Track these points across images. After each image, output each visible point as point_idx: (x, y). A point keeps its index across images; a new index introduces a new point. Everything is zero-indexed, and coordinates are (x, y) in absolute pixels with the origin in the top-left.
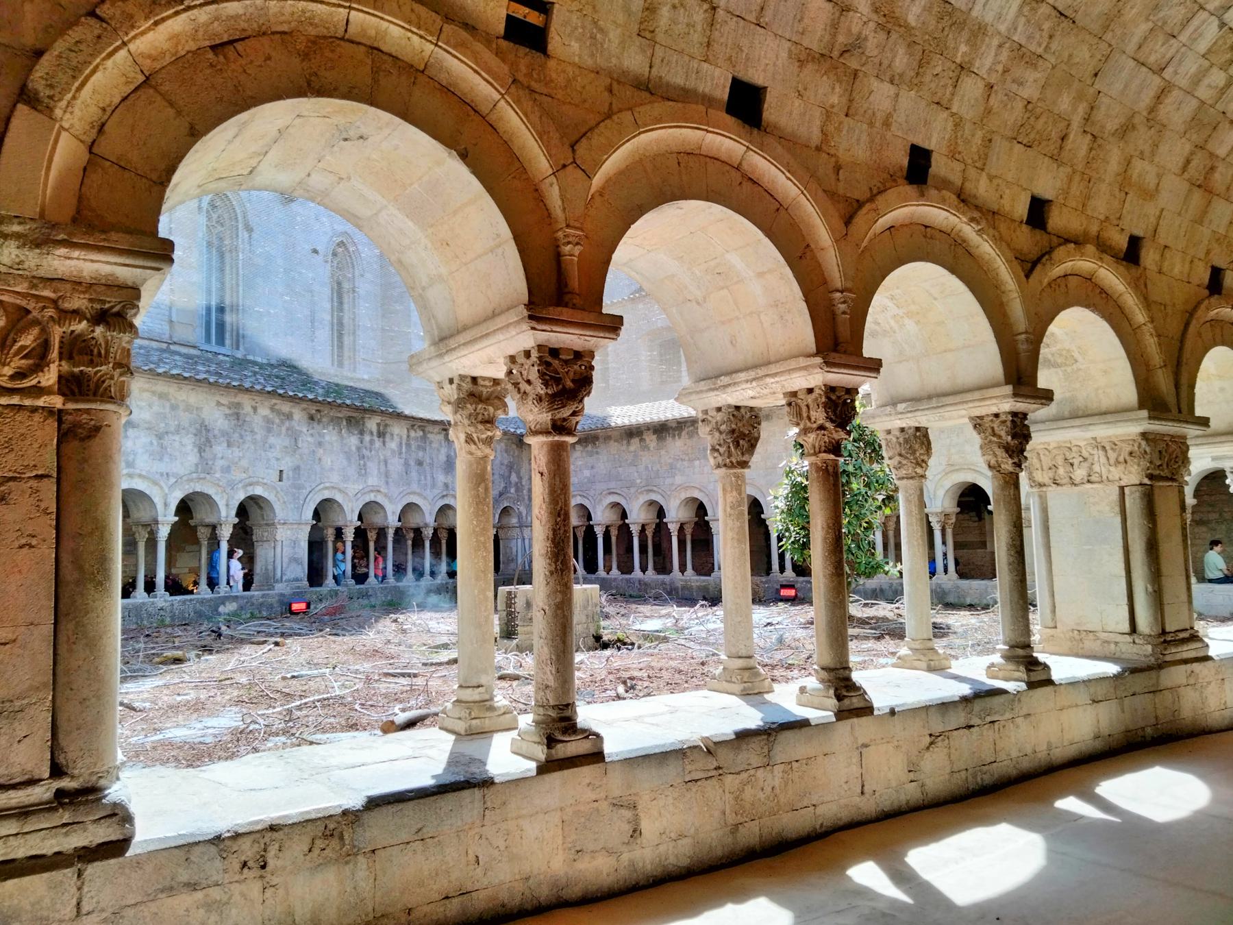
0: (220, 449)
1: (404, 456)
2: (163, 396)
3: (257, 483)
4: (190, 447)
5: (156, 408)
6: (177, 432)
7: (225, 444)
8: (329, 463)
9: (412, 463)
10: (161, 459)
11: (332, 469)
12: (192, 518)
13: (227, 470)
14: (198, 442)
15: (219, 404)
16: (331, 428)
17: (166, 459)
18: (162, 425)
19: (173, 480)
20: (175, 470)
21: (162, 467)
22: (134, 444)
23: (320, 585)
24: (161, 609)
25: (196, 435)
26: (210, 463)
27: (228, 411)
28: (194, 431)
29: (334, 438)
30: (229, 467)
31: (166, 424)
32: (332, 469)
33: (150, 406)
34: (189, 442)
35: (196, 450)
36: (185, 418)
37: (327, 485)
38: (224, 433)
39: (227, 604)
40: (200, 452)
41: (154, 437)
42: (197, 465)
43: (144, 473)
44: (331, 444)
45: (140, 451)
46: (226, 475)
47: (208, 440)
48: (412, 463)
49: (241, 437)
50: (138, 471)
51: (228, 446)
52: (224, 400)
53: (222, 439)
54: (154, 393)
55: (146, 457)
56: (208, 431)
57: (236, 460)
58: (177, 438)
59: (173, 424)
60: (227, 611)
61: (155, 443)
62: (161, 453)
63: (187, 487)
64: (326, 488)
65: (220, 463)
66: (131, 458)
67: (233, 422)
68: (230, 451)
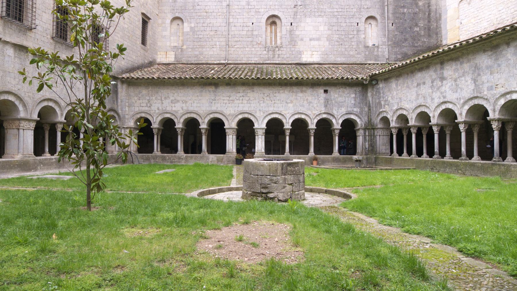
0: (484, 78)
3: (511, 92)
4: (469, 81)
6: (463, 75)
14: (474, 77)
17: (459, 91)
19: (462, 101)
20: (463, 95)
22: (446, 87)
26: (480, 86)
30: (492, 86)
35: (473, 82)
40: (475, 83)
41: (453, 82)
42: (473, 90)
43: (449, 100)
45: (448, 90)
46: (491, 92)
50: (446, 100)
51: (491, 74)
53: (487, 71)
55: (450, 92)
56: (479, 69)
58: (463, 78)
61: (454, 84)
62: (456, 89)
65: (486, 85)
66: (444, 95)
68: (492, 77)
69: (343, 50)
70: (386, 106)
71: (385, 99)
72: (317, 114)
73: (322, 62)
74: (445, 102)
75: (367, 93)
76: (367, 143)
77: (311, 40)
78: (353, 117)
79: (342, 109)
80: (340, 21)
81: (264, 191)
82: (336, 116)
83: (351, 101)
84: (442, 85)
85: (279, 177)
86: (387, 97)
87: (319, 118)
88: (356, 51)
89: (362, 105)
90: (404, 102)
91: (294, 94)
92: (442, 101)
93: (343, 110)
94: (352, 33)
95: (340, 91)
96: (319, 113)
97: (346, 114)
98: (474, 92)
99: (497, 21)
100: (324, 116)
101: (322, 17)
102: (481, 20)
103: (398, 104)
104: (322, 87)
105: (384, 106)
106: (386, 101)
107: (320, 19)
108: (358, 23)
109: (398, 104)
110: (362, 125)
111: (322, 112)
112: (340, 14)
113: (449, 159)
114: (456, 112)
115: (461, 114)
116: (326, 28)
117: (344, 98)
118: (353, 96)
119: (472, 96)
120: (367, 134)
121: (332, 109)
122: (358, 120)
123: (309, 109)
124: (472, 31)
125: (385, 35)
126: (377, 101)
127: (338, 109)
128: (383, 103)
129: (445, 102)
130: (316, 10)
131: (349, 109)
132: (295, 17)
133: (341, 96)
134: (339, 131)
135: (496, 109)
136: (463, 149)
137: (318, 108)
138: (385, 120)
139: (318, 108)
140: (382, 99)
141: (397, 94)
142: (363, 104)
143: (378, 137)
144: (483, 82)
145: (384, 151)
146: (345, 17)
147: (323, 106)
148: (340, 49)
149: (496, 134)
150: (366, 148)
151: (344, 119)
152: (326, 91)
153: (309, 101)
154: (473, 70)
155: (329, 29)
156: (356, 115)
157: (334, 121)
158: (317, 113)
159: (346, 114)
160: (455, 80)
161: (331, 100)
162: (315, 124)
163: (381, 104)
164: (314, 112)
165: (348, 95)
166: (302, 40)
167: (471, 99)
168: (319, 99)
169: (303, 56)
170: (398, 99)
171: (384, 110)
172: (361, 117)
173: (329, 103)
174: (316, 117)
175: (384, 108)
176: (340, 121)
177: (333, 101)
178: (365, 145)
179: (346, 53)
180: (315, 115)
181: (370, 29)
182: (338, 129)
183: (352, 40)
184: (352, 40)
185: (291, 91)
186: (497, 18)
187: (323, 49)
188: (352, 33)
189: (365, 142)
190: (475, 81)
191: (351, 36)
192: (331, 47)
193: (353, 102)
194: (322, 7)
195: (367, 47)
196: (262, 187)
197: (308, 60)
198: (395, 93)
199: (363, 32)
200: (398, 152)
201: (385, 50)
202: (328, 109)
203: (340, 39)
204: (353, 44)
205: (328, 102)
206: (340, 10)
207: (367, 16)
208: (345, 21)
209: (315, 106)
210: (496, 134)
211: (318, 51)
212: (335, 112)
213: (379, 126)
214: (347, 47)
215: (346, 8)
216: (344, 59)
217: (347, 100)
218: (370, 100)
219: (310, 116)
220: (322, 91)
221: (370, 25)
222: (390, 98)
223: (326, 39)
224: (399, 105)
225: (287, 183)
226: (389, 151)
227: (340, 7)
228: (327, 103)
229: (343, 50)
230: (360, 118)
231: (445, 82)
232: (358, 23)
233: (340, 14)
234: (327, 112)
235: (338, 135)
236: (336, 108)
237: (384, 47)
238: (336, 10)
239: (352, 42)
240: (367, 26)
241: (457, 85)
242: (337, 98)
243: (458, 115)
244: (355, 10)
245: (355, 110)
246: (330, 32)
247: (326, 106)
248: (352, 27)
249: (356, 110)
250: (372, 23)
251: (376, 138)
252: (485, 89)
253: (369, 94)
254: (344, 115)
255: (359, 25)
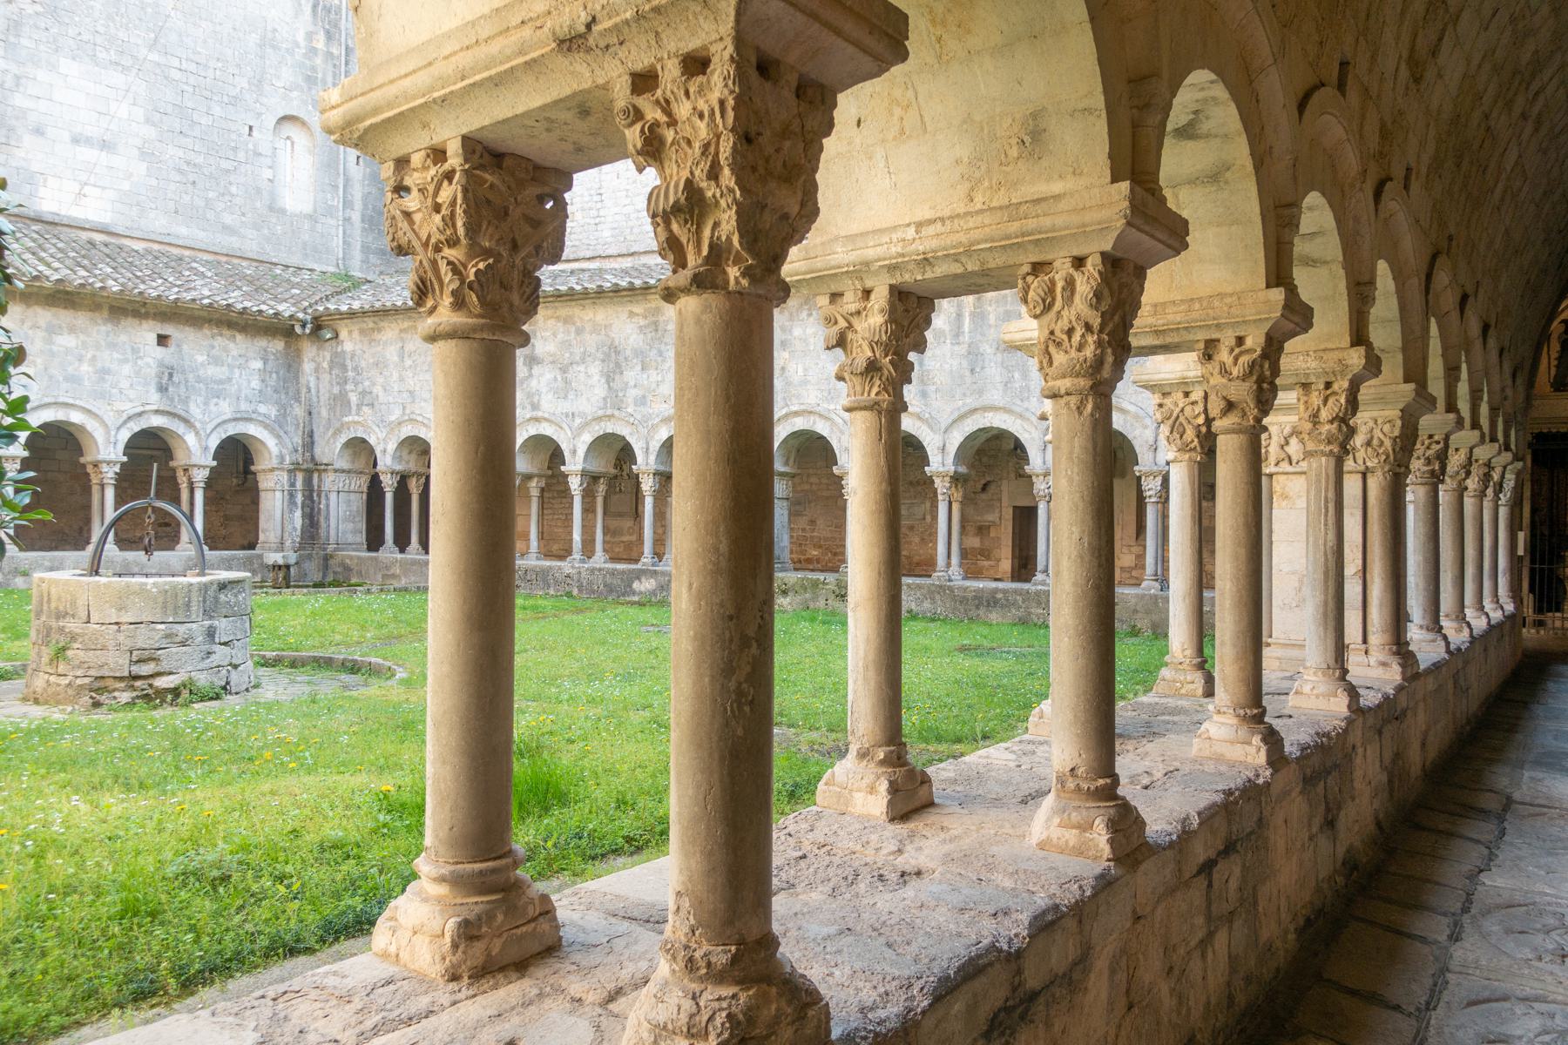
0: (631, 375)
1: (966, 338)
2: (567, 320)
4: (596, 378)
5: (560, 336)
6: (583, 361)
7: (639, 367)
8: (800, 372)
9: (988, 349)
10: (565, 397)
11: (805, 383)
12: (564, 464)
13: (641, 401)
15: (632, 314)
16: (804, 314)
17: (571, 396)
18: (567, 355)
19: (578, 421)
20: (581, 409)
21: (565, 406)
23: (1028, 580)
24: (568, 576)
25: (603, 361)
26: (621, 394)
27: (642, 322)
28: (602, 356)
29: (810, 331)
30: (644, 397)
31: (571, 354)
32: (805, 383)
33: (555, 335)
34: (595, 369)
35: (603, 380)
36: (591, 340)
37: (794, 408)
38: (638, 353)
39: (643, 579)
40: (608, 382)
41: (558, 372)
42: (604, 399)
43: (546, 415)
44: (804, 340)
45: (544, 390)
46: (642, 408)
47: (618, 365)
48: (988, 349)
49: (660, 353)
50: (540, 414)
52: (638, 309)
54: (558, 318)
55: (550, 396)
56: (617, 353)
57: (654, 386)
58: (582, 368)
59: (578, 351)
60: (643, 589)
62: (565, 390)
63: (597, 428)
64: (797, 414)
66: (535, 400)
67: (649, 336)
68: (645, 376)
69: (200, 203)
70: (365, 409)
71: (360, 389)
72: (131, 412)
73: (120, 230)
74: (537, 420)
75: (300, 363)
76: (298, 513)
77: (76, 140)
78: (252, 430)
79: (221, 402)
80: (190, 104)
81: (146, 669)
82: (198, 425)
83: (249, 382)
84: (531, 375)
85: (194, 626)
86: (367, 383)
87: (136, 427)
88: (243, 214)
89: (283, 397)
90: (423, 404)
91: (40, 334)
92: (528, 416)
93: (225, 409)
94: (231, 154)
95: (216, 344)
96: (142, 409)
97: (235, 420)
98: (606, 404)
99: (631, 233)
100: (157, 421)
101: (125, 69)
102: (597, 220)
103: (404, 408)
104: (151, 323)
105: (359, 406)
106: (364, 393)
107: (118, 79)
108: (251, 128)
109: (404, 408)
110: (282, 458)
111: (148, 408)
112: (192, 80)
113: (538, 559)
114: (563, 446)
115: (574, 452)
116: (139, 113)
117: (225, 369)
118: (258, 364)
119: (600, 413)
120: (299, 484)
121: (186, 401)
122: (271, 442)
123: (101, 395)
124: (577, 243)
125: (336, 187)
126: (336, 390)
127: (206, 404)
128: (353, 398)
129: (537, 420)
130: (99, 40)
131: (244, 406)
132: (12, 39)
133: (216, 361)
134: (207, 472)
135: (651, 449)
136: (577, 536)
137: (132, 394)
138: (359, 447)
139: (132, 394)
140: (349, 387)
141: (402, 379)
142: (287, 393)
143: (333, 496)
144: (627, 384)
145: (350, 538)
146: (208, 94)
147: (153, 389)
148: (187, 198)
149: (649, 503)
150: (295, 529)
151: (224, 436)
152: (162, 340)
153: (99, 365)
154: (604, 353)
155: (148, 121)
156: (266, 426)
157: (190, 439)
158: (130, 408)
159: (235, 420)
160: (564, 370)
161: (183, 372)
162: (121, 447)
163: (349, 402)
164: (119, 406)
165: (241, 361)
166: (39, 131)
167: (599, 419)
168: (139, 362)
169: (42, 192)
170: (405, 395)
171: (356, 418)
172: (282, 434)
173: (175, 379)
174: (125, 422)
175: (358, 414)
176: (214, 443)
177: (191, 376)
178: (292, 520)
179: (210, 215)
180: (125, 416)
181: (289, 155)
182: (204, 467)
183: (232, 178)
184: (232, 178)
185: (28, 324)
186: (632, 228)
187: (126, 186)
188: (231, 154)
189: (291, 511)
190: (609, 380)
191: (225, 164)
192: (154, 182)
193: (256, 384)
194: (122, 34)
195: (275, 209)
196: (134, 659)
197: (63, 213)
198: (395, 375)
199: (269, 161)
200: (396, 542)
201: (333, 231)
202: (172, 400)
203: (188, 163)
204: (234, 189)
205: (171, 375)
206: (193, 67)
207: (282, 114)
208: (209, 108)
209: (121, 385)
210: (649, 503)
211: (104, 188)
212: (195, 411)
213: (343, 464)
214: (211, 195)
215: (212, 64)
216: (201, 235)
217: (237, 375)
218: (312, 385)
219: (106, 418)
220: (152, 338)
221: (288, 142)
222: (378, 390)
223: (136, 152)
224: (408, 412)
225: (217, 640)
226: (362, 538)
227: (191, 56)
228: (167, 380)
229: (200, 203)
230: (278, 437)
231: (536, 370)
232: (251, 128)
233: (192, 80)
234: (168, 409)
235: (202, 485)
236: (200, 400)
237: (332, 222)
238: (176, 63)
239: (231, 184)
240: (280, 144)
241: (566, 381)
242: (202, 364)
243: (567, 454)
244: (246, 86)
245: (262, 409)
246: (150, 132)
247: (162, 389)
248: (234, 136)
249: (268, 410)
250: (295, 138)
251: (327, 499)
252: (630, 400)
253: (308, 367)
254: (224, 422)
255: (255, 133)
